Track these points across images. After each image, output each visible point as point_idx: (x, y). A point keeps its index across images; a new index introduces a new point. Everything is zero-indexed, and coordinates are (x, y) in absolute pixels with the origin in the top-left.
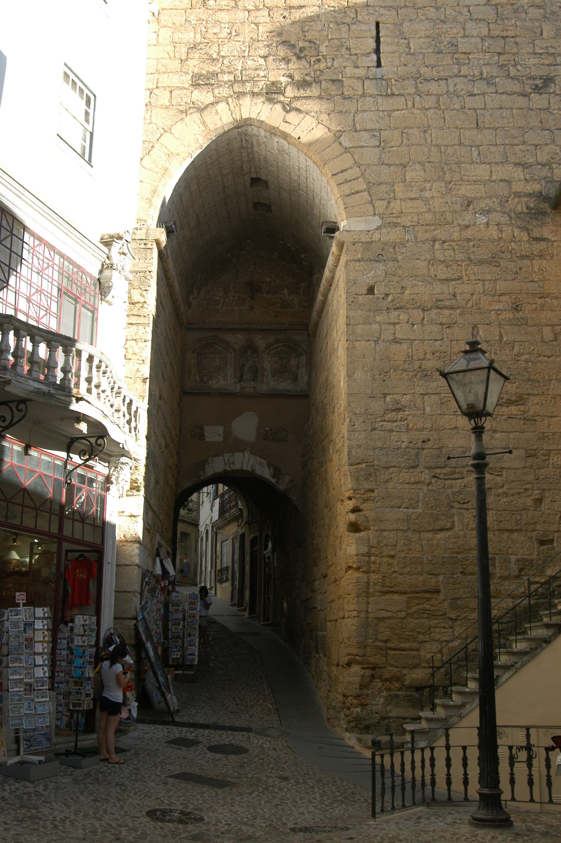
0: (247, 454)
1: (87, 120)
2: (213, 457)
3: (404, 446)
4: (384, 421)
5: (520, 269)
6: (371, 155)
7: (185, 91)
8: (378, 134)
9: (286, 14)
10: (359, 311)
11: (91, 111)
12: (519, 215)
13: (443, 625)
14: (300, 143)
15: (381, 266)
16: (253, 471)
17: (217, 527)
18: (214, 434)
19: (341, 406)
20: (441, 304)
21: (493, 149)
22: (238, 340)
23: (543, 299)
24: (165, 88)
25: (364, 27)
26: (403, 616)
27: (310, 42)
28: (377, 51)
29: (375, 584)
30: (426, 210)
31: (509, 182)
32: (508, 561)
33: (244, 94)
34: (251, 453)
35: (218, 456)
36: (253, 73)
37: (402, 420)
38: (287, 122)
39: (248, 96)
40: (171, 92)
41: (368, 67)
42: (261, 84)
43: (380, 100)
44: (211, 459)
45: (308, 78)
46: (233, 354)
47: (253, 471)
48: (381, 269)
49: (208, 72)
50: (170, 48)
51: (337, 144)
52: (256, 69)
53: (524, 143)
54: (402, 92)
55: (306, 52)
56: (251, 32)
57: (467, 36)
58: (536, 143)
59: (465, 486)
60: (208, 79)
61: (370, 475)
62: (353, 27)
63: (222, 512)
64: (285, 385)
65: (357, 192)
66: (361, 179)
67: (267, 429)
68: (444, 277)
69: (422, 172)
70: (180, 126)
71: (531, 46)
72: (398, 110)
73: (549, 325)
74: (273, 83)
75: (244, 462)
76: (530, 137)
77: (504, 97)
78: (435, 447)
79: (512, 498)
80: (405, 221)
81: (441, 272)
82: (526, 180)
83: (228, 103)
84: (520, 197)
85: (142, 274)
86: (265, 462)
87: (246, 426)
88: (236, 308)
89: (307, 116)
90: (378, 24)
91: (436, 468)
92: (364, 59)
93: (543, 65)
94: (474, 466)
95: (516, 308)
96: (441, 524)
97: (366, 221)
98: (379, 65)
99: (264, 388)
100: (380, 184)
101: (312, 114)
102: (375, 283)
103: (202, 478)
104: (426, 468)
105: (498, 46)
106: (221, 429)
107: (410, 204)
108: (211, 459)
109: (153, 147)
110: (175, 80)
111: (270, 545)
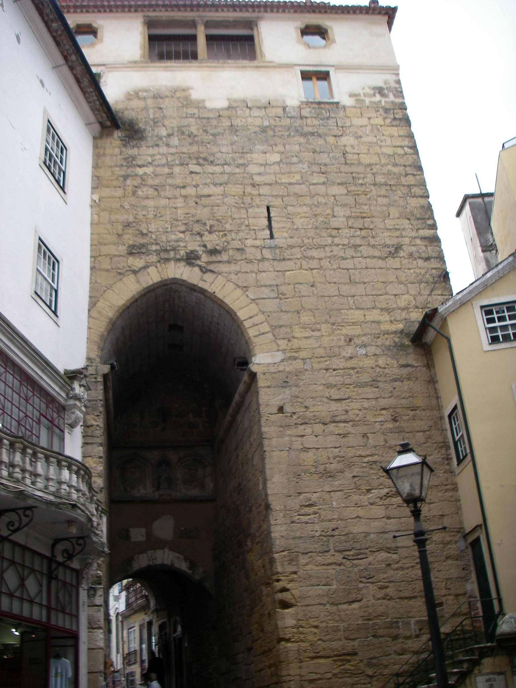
0: (166, 550)
1: (53, 281)
3: (317, 534)
4: (300, 515)
5: (395, 388)
6: (271, 305)
7: (122, 258)
8: (275, 289)
9: (197, 200)
10: (273, 428)
11: (56, 273)
12: (388, 348)
13: (363, 681)
14: (215, 296)
15: (287, 391)
17: (124, 617)
18: (138, 534)
19: (260, 505)
20: (338, 419)
21: (365, 298)
23: (413, 412)
24: (106, 256)
25: (257, 210)
26: (329, 677)
27: (218, 220)
28: (270, 227)
29: (305, 651)
30: (318, 346)
31: (378, 322)
32: (408, 624)
33: (168, 260)
34: (170, 549)
36: (175, 244)
37: (315, 513)
38: (205, 281)
39: (173, 261)
40: (111, 259)
41: (264, 239)
42: (182, 253)
43: (275, 263)
45: (218, 248)
48: (288, 392)
49: (140, 244)
50: (109, 226)
51: (244, 296)
52: (178, 241)
53: (386, 293)
54: (291, 257)
55: (215, 229)
56: (171, 214)
57: (335, 217)
58: (395, 293)
59: (370, 564)
60: (140, 249)
61: (291, 560)
62: (250, 210)
63: (128, 605)
64: (194, 492)
65: (263, 334)
66: (265, 324)
67: (182, 529)
68: (337, 397)
69: (312, 318)
70: (119, 285)
71: (383, 223)
72: (289, 271)
73: (421, 432)
74: (192, 252)
75: (165, 557)
76: (391, 289)
77: (368, 260)
78: (342, 534)
79: (407, 571)
80: (303, 354)
81: (335, 394)
82: (391, 321)
83: (156, 267)
84: (388, 334)
85: (94, 402)
87: (164, 527)
89: (220, 276)
90: (268, 208)
91: (344, 551)
92: (261, 233)
93: (393, 237)
94: (415, 541)
95: (395, 420)
96: (353, 596)
97: (273, 356)
98: (272, 237)
100: (281, 326)
101: (224, 274)
102: (284, 404)
104: (336, 551)
105: (359, 224)
106: (143, 531)
107: (305, 342)
109: (98, 301)
110: (113, 250)
111: (179, 629)
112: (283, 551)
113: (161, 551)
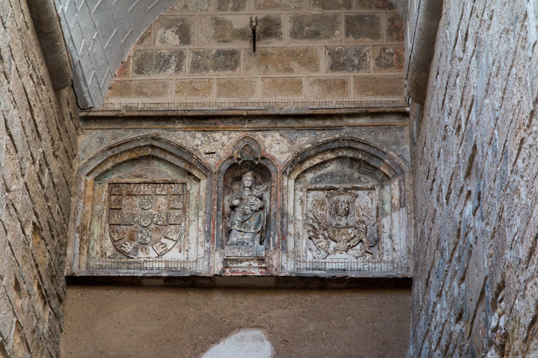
22: (217, 146)
46: (204, 183)
99: (287, 266)
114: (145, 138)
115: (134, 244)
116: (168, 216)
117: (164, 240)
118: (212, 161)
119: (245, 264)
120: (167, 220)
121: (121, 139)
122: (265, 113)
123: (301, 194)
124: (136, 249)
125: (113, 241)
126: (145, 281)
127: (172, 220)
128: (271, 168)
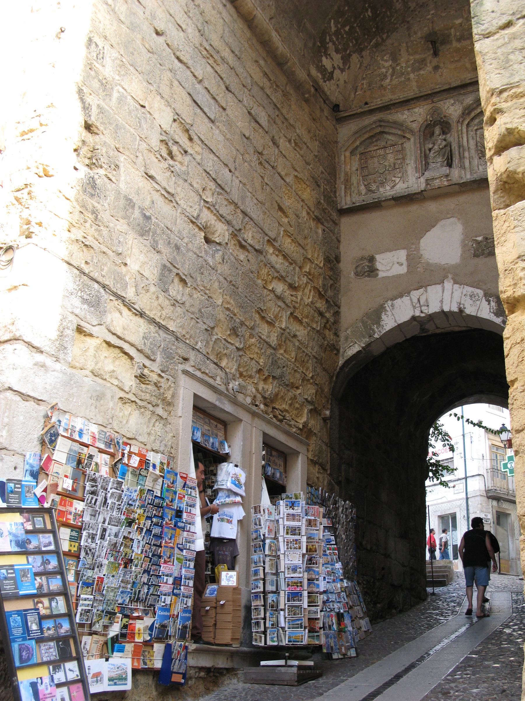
0: (448, 285)
2: (392, 300)
16: (461, 311)
18: (391, 264)
34: (455, 282)
35: (401, 296)
44: (390, 303)
47: (461, 311)
67: (480, 239)
86: (481, 293)
88: (412, 76)
103: (376, 336)
106: (402, 255)
108: (390, 303)
112: (508, 25)
113: (439, 287)
114: (375, 122)
115: (377, 184)
116: (394, 164)
117: (394, 179)
118: (414, 126)
119: (437, 181)
120: (394, 167)
121: (361, 126)
122: (442, 89)
123: (472, 133)
124: (378, 187)
125: (365, 185)
126: (383, 204)
127: (397, 166)
128: (450, 121)
